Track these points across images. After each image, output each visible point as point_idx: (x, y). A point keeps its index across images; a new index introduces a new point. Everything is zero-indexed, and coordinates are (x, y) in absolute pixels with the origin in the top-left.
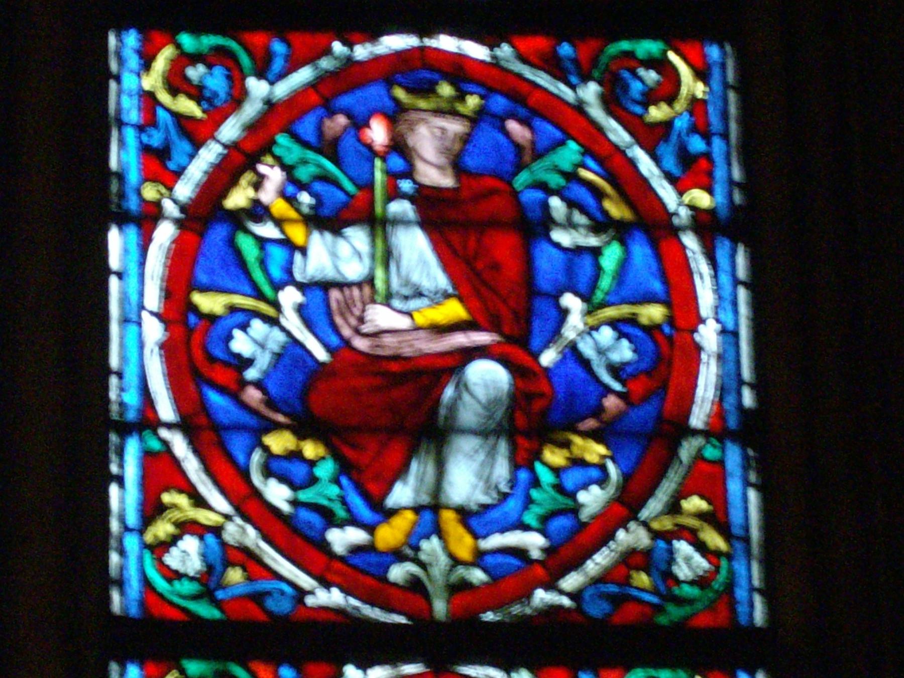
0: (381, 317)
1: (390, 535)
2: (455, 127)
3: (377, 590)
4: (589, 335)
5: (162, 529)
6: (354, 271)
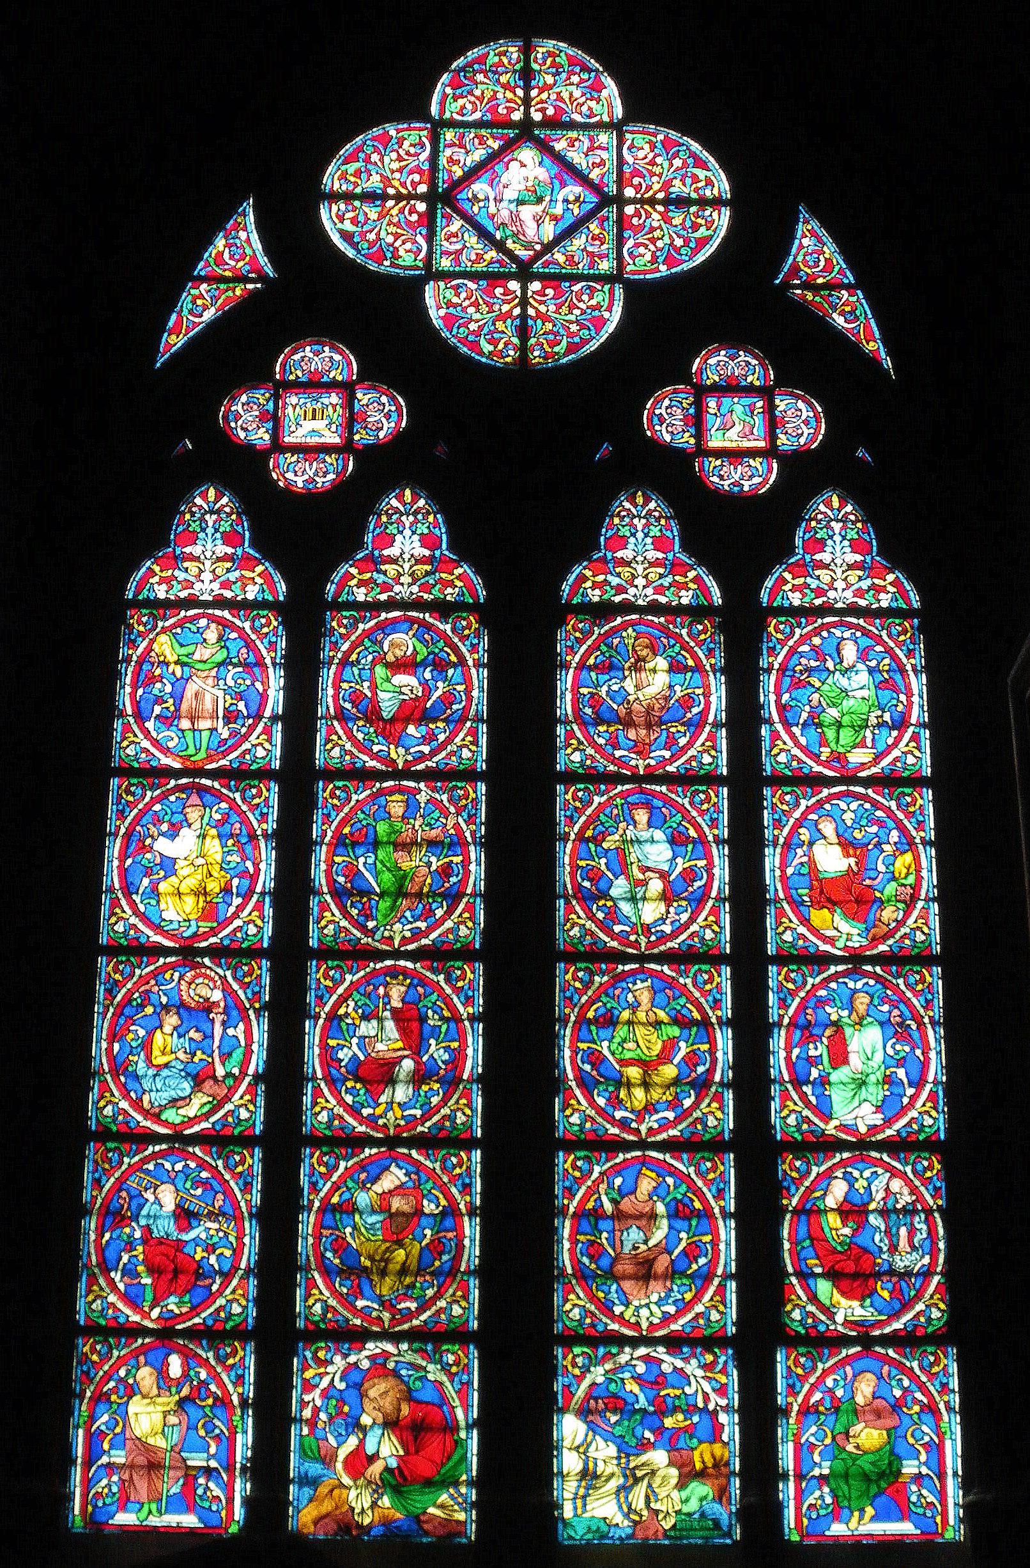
0: (380, 1046)
1: (379, 1111)
2: (403, 989)
3: (376, 1128)
4: (437, 1052)
5: (317, 1109)
6: (373, 1033)
